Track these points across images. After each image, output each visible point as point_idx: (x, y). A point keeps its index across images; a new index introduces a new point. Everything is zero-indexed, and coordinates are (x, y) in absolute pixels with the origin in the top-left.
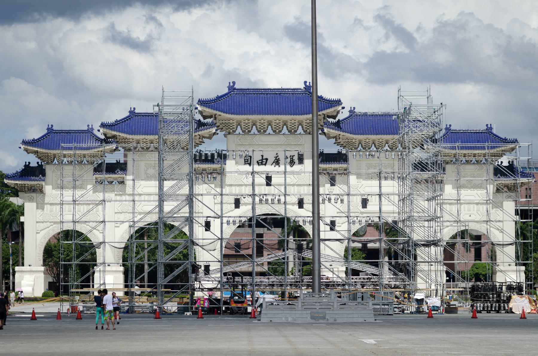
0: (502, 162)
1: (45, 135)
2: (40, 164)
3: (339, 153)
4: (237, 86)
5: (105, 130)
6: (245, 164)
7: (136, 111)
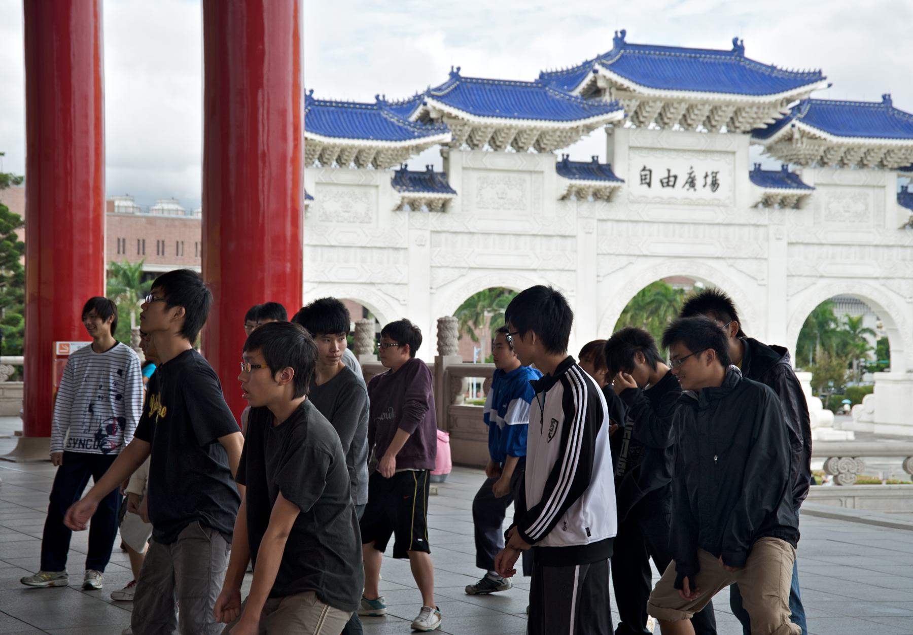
4: (628, 39)
6: (642, 184)
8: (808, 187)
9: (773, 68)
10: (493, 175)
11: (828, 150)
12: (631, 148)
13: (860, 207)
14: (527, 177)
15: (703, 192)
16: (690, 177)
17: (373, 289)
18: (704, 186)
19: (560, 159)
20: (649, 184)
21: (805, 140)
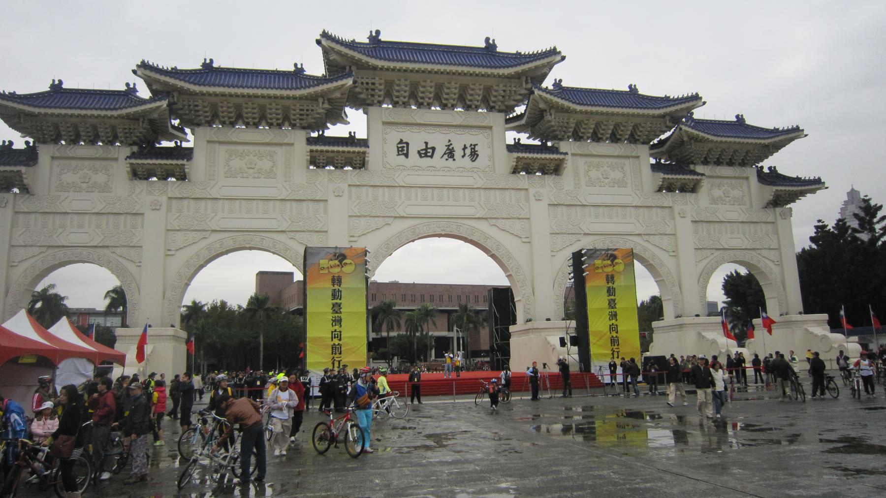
0: (762, 167)
1: (43, 93)
2: (31, 144)
3: (544, 145)
4: (383, 38)
5: (148, 72)
6: (399, 155)
7: (215, 65)
8: (561, 153)
9: (518, 54)
10: (240, 148)
11: (578, 124)
12: (384, 123)
13: (617, 175)
14: (278, 150)
15: (462, 161)
16: (448, 149)
17: (106, 252)
18: (463, 157)
19: (315, 135)
20: (407, 155)
21: (553, 111)
